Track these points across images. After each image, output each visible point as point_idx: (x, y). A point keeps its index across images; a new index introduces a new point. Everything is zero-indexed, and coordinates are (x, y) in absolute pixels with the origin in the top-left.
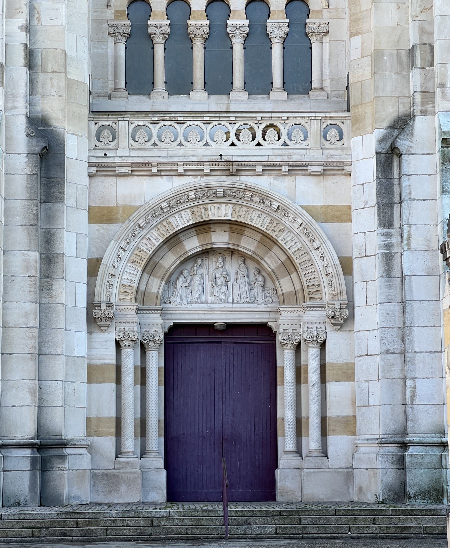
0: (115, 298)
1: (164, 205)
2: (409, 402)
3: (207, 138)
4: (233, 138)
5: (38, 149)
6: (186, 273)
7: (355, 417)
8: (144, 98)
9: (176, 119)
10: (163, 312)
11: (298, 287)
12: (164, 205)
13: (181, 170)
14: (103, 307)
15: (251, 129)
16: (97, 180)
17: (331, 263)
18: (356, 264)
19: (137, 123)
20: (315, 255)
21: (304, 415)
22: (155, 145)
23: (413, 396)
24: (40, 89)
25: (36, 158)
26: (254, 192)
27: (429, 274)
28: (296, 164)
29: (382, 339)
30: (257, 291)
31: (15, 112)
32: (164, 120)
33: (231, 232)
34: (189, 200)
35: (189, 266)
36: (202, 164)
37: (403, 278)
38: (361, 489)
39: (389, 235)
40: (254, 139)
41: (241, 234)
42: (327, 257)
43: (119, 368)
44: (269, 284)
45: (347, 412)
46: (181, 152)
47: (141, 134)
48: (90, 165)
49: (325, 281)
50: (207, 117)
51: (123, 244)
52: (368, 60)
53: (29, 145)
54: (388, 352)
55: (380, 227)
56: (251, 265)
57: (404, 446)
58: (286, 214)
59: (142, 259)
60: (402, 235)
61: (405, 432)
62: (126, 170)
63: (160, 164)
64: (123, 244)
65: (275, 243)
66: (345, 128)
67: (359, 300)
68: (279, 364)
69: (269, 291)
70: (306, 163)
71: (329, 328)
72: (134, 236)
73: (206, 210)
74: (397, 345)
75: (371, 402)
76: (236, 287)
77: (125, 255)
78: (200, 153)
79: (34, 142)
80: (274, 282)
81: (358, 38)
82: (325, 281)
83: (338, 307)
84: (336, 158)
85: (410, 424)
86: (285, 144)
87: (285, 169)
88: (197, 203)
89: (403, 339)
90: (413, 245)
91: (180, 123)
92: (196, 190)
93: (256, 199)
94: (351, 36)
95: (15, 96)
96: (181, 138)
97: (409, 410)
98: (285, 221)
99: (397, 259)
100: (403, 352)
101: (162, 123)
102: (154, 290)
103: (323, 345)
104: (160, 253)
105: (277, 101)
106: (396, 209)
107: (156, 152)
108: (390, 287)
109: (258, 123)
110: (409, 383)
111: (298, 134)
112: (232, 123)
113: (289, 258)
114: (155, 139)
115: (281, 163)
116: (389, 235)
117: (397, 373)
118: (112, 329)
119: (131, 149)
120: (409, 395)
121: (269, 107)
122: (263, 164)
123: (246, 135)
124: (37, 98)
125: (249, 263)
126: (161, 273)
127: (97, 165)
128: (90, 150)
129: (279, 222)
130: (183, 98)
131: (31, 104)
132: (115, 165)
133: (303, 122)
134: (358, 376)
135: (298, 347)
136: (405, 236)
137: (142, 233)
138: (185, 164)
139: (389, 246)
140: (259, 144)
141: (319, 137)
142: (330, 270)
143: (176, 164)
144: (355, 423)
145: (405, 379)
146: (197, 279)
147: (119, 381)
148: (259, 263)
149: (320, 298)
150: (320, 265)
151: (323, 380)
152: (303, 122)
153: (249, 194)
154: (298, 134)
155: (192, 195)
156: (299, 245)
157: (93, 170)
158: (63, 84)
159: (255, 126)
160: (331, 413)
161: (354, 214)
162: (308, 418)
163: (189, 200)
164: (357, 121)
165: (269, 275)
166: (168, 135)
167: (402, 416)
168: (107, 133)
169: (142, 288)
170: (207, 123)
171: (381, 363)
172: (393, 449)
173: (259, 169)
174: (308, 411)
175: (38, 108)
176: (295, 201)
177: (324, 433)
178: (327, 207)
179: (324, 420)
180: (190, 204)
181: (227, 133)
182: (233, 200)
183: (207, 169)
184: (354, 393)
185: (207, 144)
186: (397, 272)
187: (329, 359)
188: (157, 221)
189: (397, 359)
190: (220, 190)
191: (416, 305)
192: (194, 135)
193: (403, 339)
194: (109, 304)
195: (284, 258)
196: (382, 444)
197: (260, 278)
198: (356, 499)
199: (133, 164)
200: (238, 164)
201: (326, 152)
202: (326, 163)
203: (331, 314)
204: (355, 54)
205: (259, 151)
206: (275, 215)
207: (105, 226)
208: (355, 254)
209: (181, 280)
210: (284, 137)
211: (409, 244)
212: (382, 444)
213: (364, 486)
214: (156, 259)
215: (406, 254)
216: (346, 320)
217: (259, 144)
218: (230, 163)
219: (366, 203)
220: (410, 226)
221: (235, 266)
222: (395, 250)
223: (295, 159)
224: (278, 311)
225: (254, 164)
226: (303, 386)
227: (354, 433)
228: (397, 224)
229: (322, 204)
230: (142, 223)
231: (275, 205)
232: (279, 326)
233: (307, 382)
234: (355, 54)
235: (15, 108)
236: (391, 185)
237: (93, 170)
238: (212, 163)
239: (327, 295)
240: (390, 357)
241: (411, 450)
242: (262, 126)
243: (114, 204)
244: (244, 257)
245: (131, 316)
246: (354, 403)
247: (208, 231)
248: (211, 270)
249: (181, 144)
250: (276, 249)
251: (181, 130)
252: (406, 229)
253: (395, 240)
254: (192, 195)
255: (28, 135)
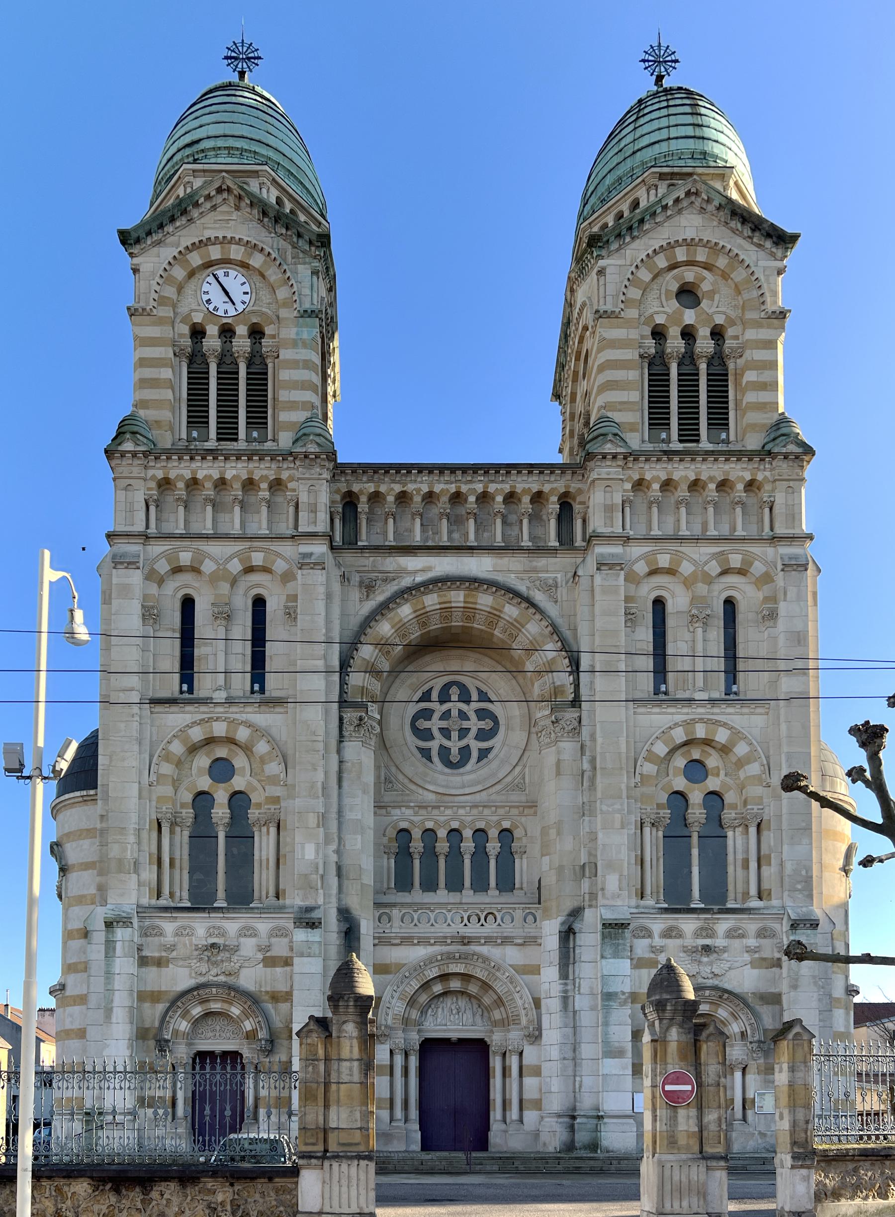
0: (389, 1022)
1: (422, 964)
2: (577, 1090)
3: (449, 921)
4: (466, 921)
5: (345, 929)
6: (433, 1006)
7: (541, 1100)
8: (406, 894)
9: (429, 908)
10: (419, 1031)
11: (505, 1016)
12: (422, 964)
13: (432, 941)
14: (383, 1028)
15: (477, 915)
16: (377, 947)
17: (527, 1001)
18: (543, 1002)
19: (404, 911)
20: (517, 996)
21: (507, 1097)
22: (415, 925)
23: (580, 1087)
24: (345, 890)
25: (343, 935)
26: (479, 956)
27: (592, 1010)
28: (506, 937)
29: (561, 1050)
30: (478, 1018)
31: (330, 905)
32: (421, 909)
33: (462, 980)
34: (437, 961)
35: (435, 1001)
36: (446, 937)
37: (575, 1012)
38: (545, 1144)
39: (566, 984)
40: (479, 921)
41: (469, 981)
42: (525, 997)
43: (392, 1067)
44: (486, 1014)
45: (536, 1096)
46: (432, 930)
47: (407, 919)
48: (374, 938)
49: (523, 1012)
50: (449, 907)
51: (395, 988)
52: (553, 871)
53: (339, 926)
54: (564, 1059)
55: (560, 979)
56: (474, 1001)
57: (574, 1118)
58: (498, 970)
59: (407, 997)
60: (574, 985)
61: (574, 1109)
62: (398, 941)
63: (419, 938)
64: (395, 988)
65: (490, 987)
66: (538, 915)
67: (545, 1024)
68: (491, 1065)
69: (485, 1019)
70: (513, 937)
71: (525, 1042)
72: (402, 983)
73: (448, 967)
74: (570, 1055)
75: (553, 1090)
76: (465, 1016)
77: (396, 995)
78: (444, 930)
79: (342, 924)
80: (489, 1013)
81: (547, 857)
82: (523, 1012)
83: (531, 1029)
84: (532, 934)
85: (578, 1104)
86: (499, 925)
87: (499, 941)
88: (442, 963)
89: (574, 1051)
90: (582, 991)
91: (432, 911)
92: (442, 955)
93: (480, 960)
94: (542, 855)
95: (330, 895)
96: (432, 921)
97: (578, 1095)
98: (498, 974)
99: (571, 999)
100: (574, 1059)
101: (420, 911)
102: (414, 1017)
103: (521, 1054)
104: (418, 994)
105: (493, 897)
106: (571, 967)
107: (416, 930)
108: (566, 1017)
109: (482, 911)
110: (578, 1079)
111: (507, 918)
112: (465, 911)
113: (499, 998)
114: (416, 921)
115: (497, 937)
116: (566, 984)
117: (570, 1072)
118: (388, 1042)
119: (401, 927)
120: (577, 1086)
121: (487, 900)
122: (485, 938)
123: (474, 919)
124: (342, 896)
125: (473, 1000)
126: (418, 1006)
127: (379, 938)
128: (374, 928)
129: (494, 975)
130: (432, 894)
131: (339, 900)
132: (390, 938)
133: (511, 911)
134: (544, 1072)
135: (504, 1054)
136: (577, 985)
137: (407, 980)
138: (435, 938)
139: (566, 991)
140: (482, 925)
141: (522, 919)
142: (526, 1006)
143: (429, 938)
144: (541, 1104)
145: (575, 1076)
146: (440, 1010)
147: (392, 1075)
148: (479, 1000)
149: (520, 1024)
150: (520, 1002)
151: (521, 1075)
152: (511, 911)
153: (476, 957)
154: (507, 918)
155: (439, 958)
156: (506, 989)
157: (376, 941)
158: (359, 887)
159: (480, 914)
160: (526, 1096)
161: (542, 970)
162: (511, 1100)
163: (437, 961)
164: (546, 910)
165: (486, 1008)
166: (424, 919)
167: (572, 1100)
168: (385, 917)
169: (406, 1016)
170: (450, 911)
171: (559, 1066)
172: (567, 1120)
173: (483, 941)
174: (511, 1095)
175: (343, 903)
176: (504, 961)
177: (521, 1109)
178: (525, 965)
179: (521, 1101)
180: (438, 964)
181: (462, 918)
182: (466, 961)
183: (449, 941)
184: (540, 1084)
185: (449, 925)
186: (571, 1008)
187: (524, 1063)
188: (417, 973)
189: (570, 1063)
190: (457, 955)
191: (583, 1029)
192: (441, 919)
193: (574, 1051)
194: (386, 1026)
195: (495, 997)
196: (559, 1116)
197: (480, 1010)
198: (541, 1150)
199: (402, 938)
200: (469, 937)
201: (526, 930)
202: (525, 937)
203: (527, 1033)
204: (545, 867)
205: (482, 930)
206: (493, 971)
207: (383, 976)
208: (543, 996)
209: (430, 1010)
210: (499, 920)
211: (579, 990)
212: (559, 1116)
213: (547, 1142)
214: (415, 997)
215: (577, 997)
216: (536, 1038)
217: (482, 925)
218: (464, 937)
219: (551, 963)
220: (580, 979)
221: (464, 1002)
222: (570, 994)
223: (505, 934)
224: (492, 1032)
225: (480, 938)
226: (507, 1080)
227: (540, 1109)
228: (571, 977)
229: (522, 963)
230: (407, 974)
231: (493, 964)
232: (492, 1041)
233: (510, 1076)
234: (545, 867)
235: (330, 903)
236: (568, 952)
237: (376, 941)
238: (452, 937)
239: (524, 1021)
240: (565, 1062)
241: (578, 1120)
242: (485, 914)
243: (388, 962)
244: (470, 996)
245: (400, 1034)
246: (541, 1090)
247: (448, 980)
248: (449, 1005)
249: (432, 925)
250: (491, 992)
251: (432, 916)
252: (577, 980)
253: (569, 987)
254: (439, 958)
255: (338, 920)
